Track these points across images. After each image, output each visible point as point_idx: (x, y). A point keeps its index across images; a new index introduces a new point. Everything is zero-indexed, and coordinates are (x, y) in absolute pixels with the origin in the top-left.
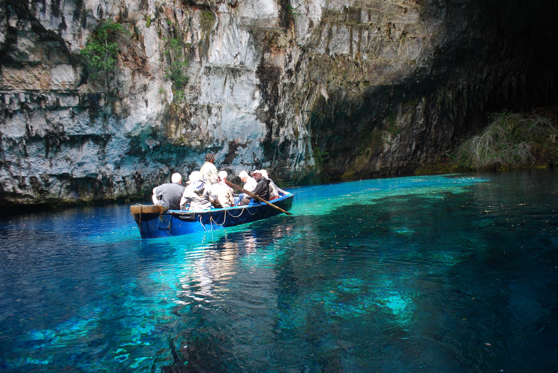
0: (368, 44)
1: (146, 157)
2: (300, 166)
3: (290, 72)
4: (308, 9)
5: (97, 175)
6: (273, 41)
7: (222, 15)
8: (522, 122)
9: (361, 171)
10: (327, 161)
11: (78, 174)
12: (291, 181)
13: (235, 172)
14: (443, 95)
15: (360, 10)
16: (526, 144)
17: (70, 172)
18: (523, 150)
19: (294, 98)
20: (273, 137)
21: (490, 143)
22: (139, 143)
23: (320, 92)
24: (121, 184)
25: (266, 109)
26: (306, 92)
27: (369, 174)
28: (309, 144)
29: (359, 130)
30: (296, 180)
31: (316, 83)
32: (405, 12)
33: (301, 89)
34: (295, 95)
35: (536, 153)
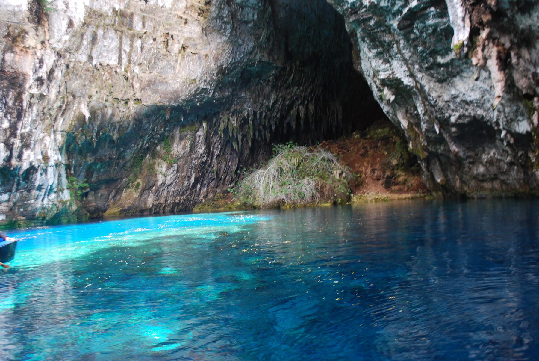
0: (141, 55)
2: (50, 200)
3: (40, 81)
6: (19, 39)
8: (307, 156)
9: (129, 209)
10: (86, 195)
12: (37, 219)
14: (227, 121)
15: (132, 15)
16: (310, 180)
18: (308, 186)
19: (44, 114)
20: (14, 162)
21: (274, 178)
23: (78, 108)
26: (61, 107)
27: (138, 212)
29: (128, 158)
30: (44, 218)
31: (74, 97)
32: (186, 23)
33: (55, 102)
34: (45, 110)
35: (320, 189)
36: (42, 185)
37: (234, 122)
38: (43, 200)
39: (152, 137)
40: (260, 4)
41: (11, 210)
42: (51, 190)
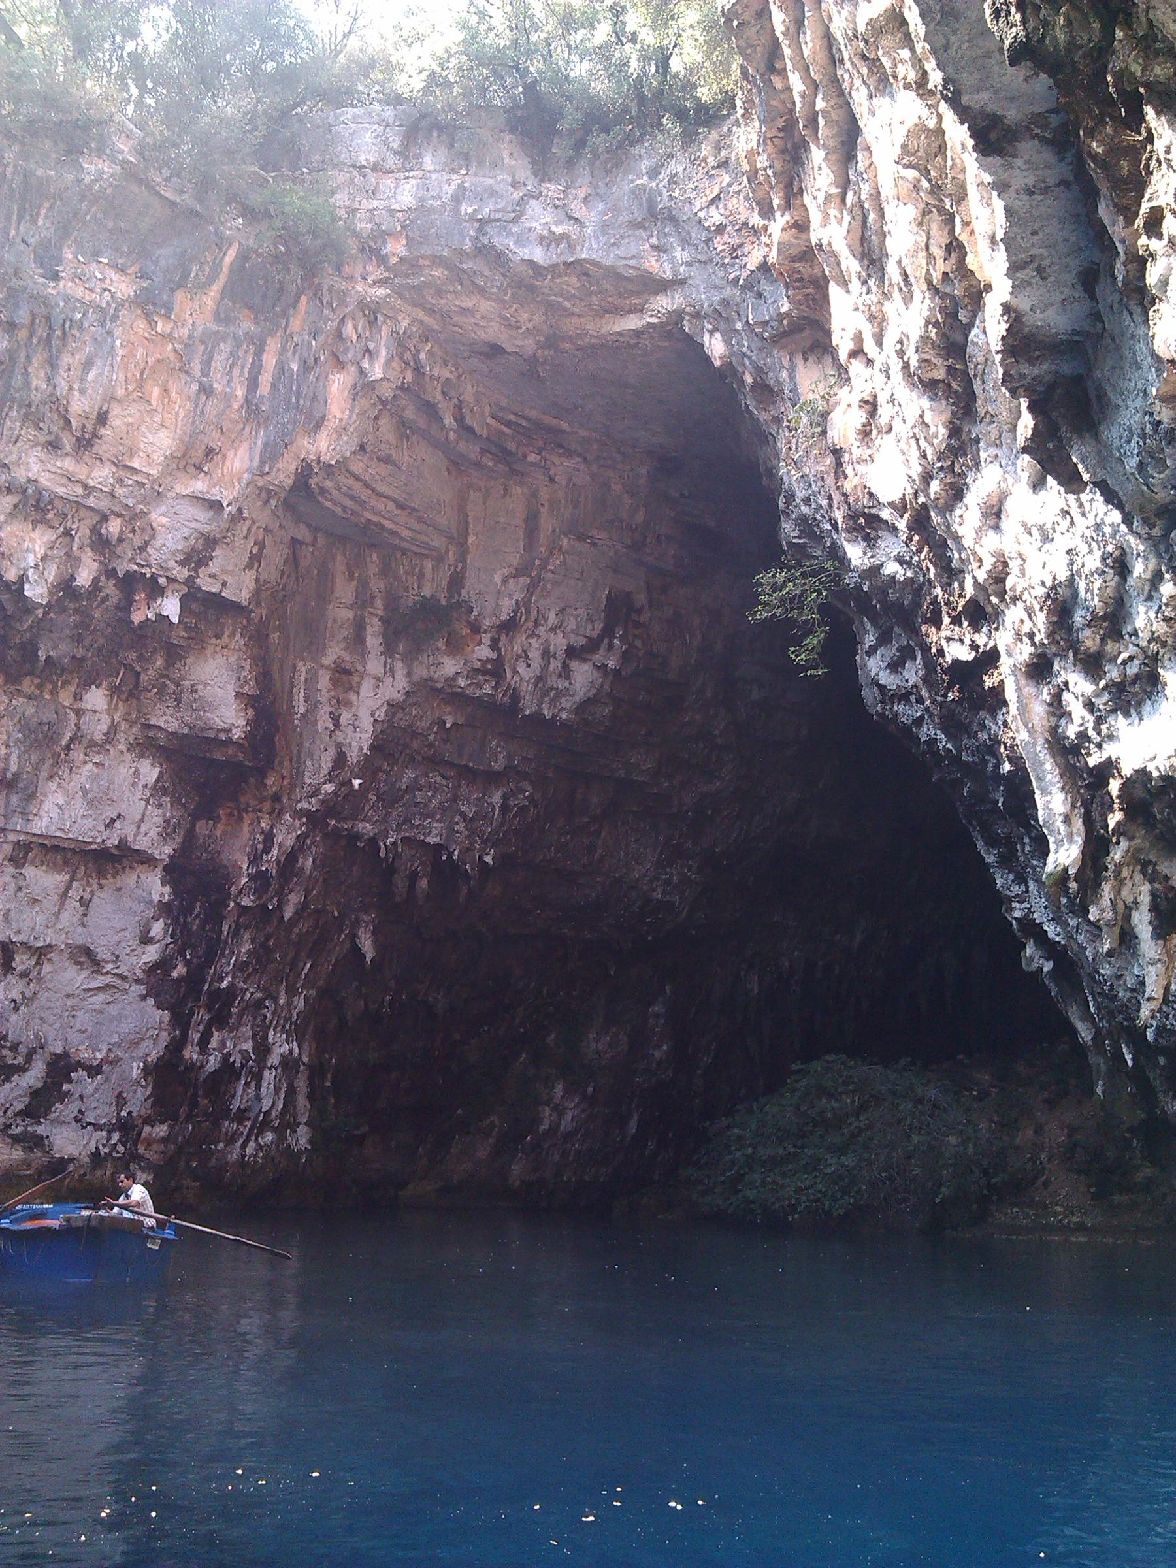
2: (259, 1147)
7: (86, 718)
13: (51, 1145)
20: (191, 1053)
23: (354, 937)
25: (179, 971)
28: (302, 1084)
36: (245, 1110)
37: (754, 986)
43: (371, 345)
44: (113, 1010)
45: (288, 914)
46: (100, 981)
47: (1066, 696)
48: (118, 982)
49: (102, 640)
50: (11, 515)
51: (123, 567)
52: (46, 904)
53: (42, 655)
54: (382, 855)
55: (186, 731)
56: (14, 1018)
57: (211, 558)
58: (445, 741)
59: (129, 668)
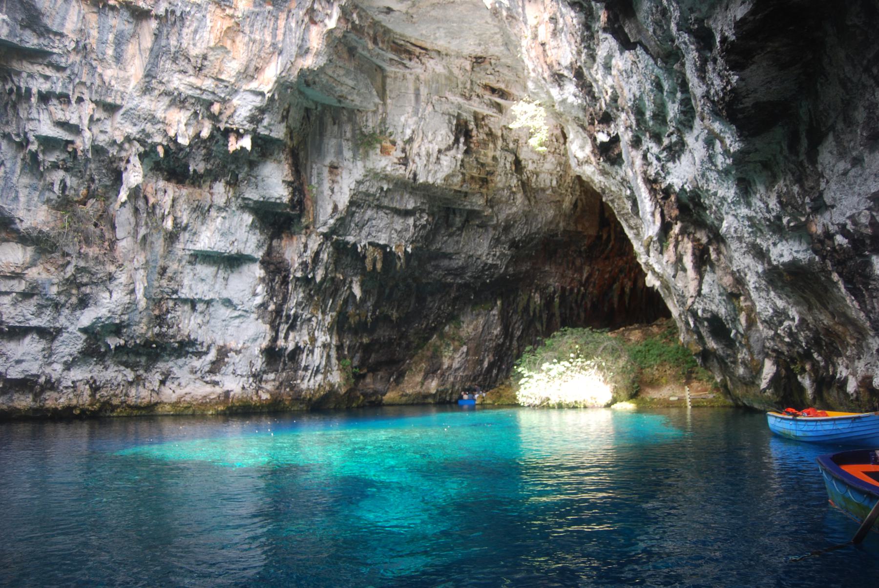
1: (107, 358)
4: (332, 190)
5: (38, 376)
11: (14, 373)
17: (4, 371)
20: (281, 343)
22: (98, 340)
23: (350, 288)
24: (70, 390)
25: (272, 307)
28: (333, 353)
38: (309, 381)
39: (439, 316)
40: (558, 169)
41: (278, 388)
42: (317, 371)
43: (329, 12)
44: (244, 326)
45: (318, 279)
46: (236, 313)
47: (649, 155)
48: (244, 313)
49: (218, 161)
50: (169, 106)
51: (222, 126)
52: (208, 281)
53: (191, 169)
54: (359, 250)
55: (262, 199)
56: (200, 331)
57: (263, 119)
58: (386, 196)
59: (233, 172)
